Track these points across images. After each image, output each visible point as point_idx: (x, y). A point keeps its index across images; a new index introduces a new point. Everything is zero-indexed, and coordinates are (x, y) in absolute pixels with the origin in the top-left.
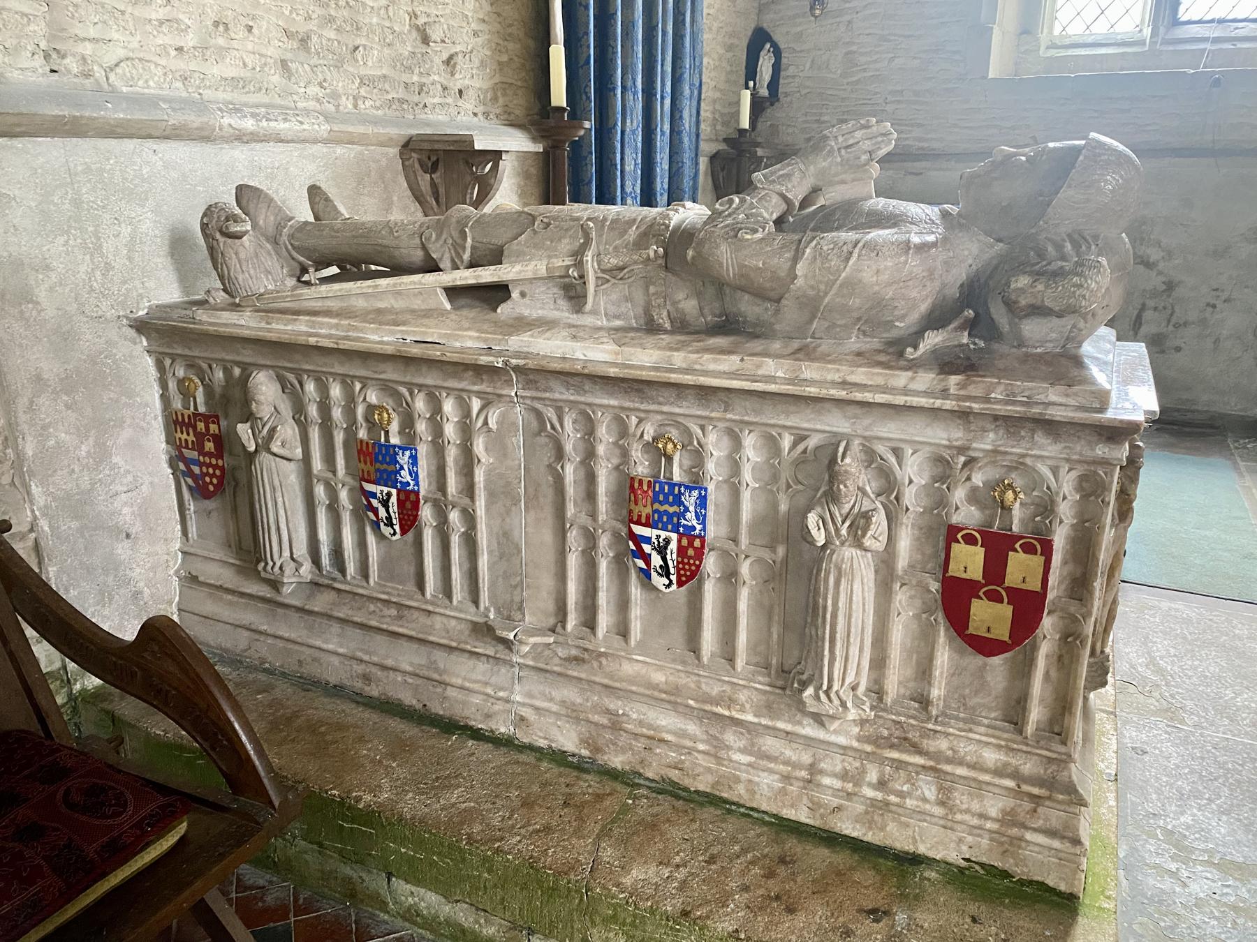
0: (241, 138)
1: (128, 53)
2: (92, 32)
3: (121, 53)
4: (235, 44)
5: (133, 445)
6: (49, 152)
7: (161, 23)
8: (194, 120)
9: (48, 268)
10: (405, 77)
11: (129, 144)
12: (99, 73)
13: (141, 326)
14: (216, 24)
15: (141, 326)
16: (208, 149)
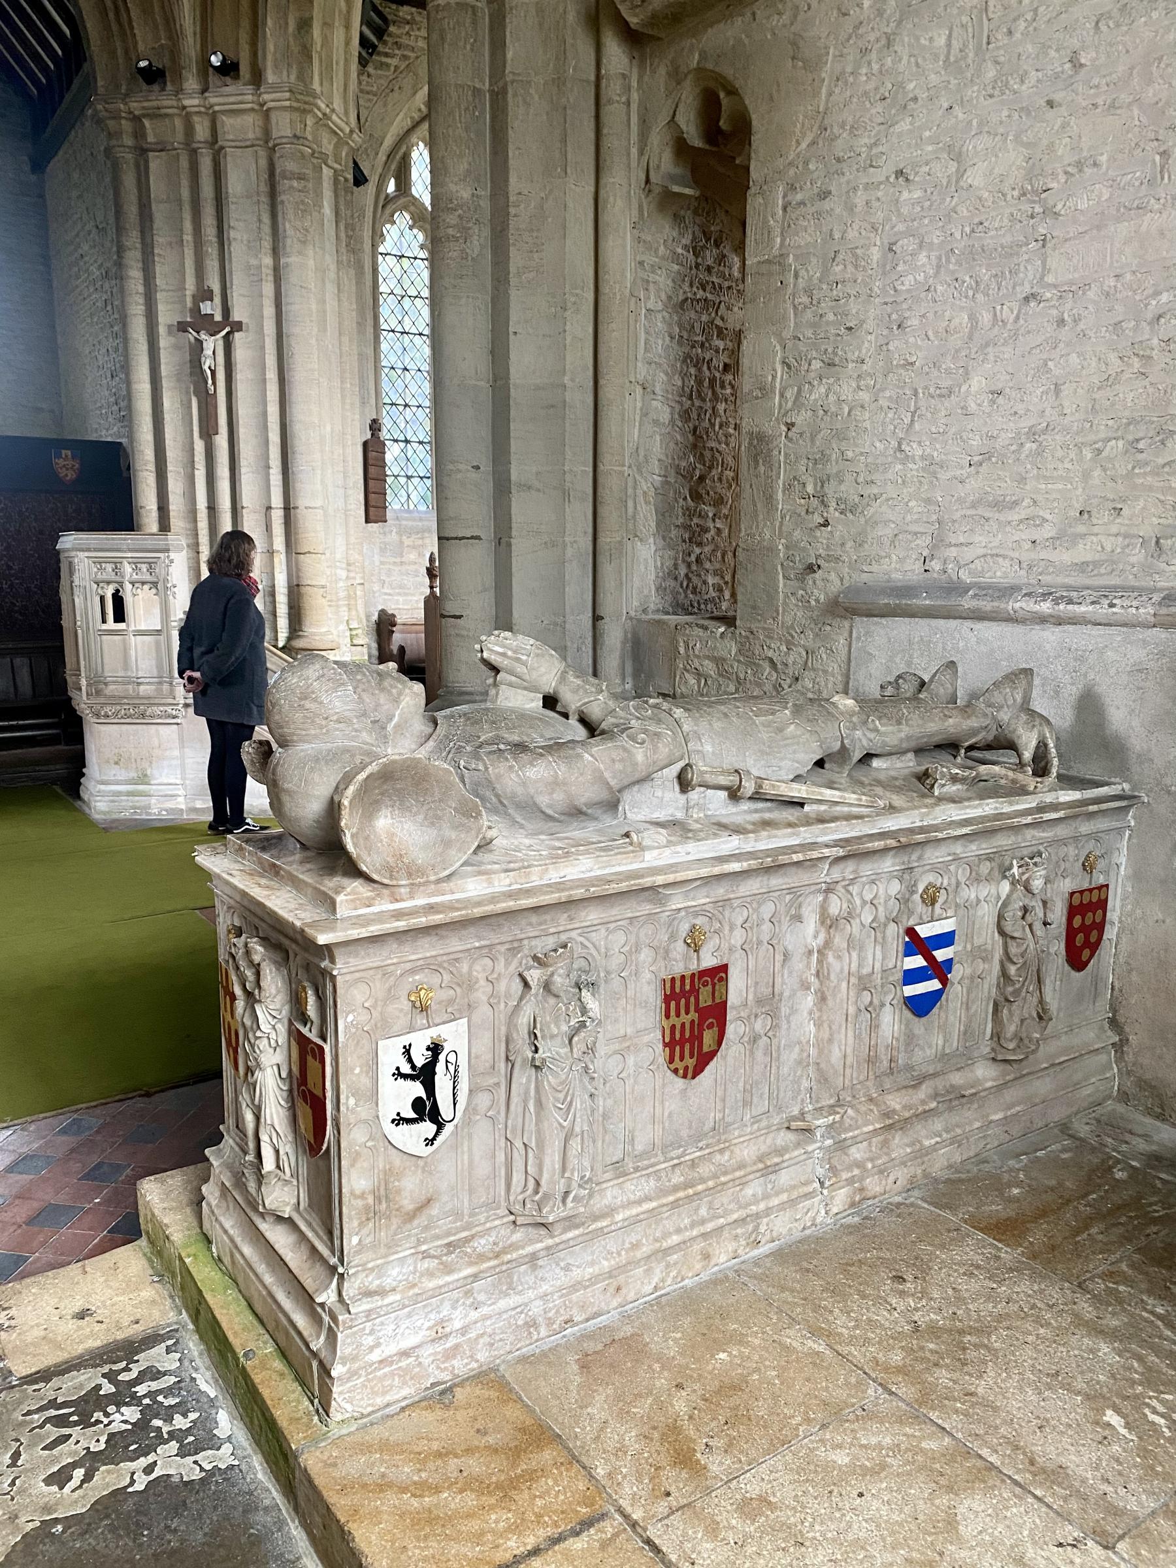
0: (1043, 620)
1: (986, 552)
2: (962, 540)
3: (981, 551)
4: (1096, 530)
6: (901, 628)
7: (1021, 521)
11: (953, 623)
16: (1019, 629)
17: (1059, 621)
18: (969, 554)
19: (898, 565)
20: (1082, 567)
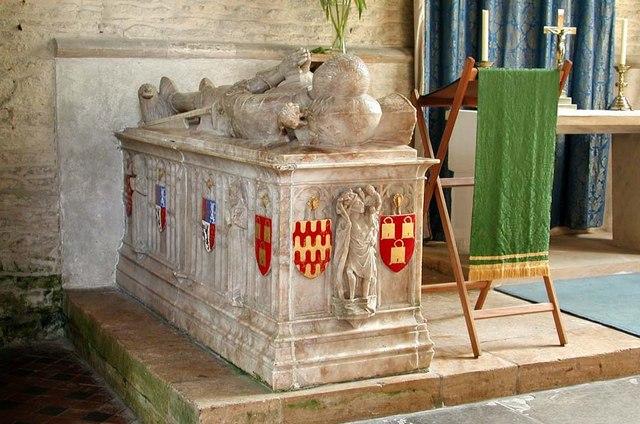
0: (182, 56)
1: (140, 22)
3: (133, 23)
5: (108, 188)
6: (93, 63)
8: (155, 49)
9: (84, 108)
10: (307, 24)
12: (119, 32)
13: (119, 136)
14: (184, 7)
15: (119, 136)
17: (190, 56)
18: (127, 24)
19: (85, 28)
20: (189, 32)
